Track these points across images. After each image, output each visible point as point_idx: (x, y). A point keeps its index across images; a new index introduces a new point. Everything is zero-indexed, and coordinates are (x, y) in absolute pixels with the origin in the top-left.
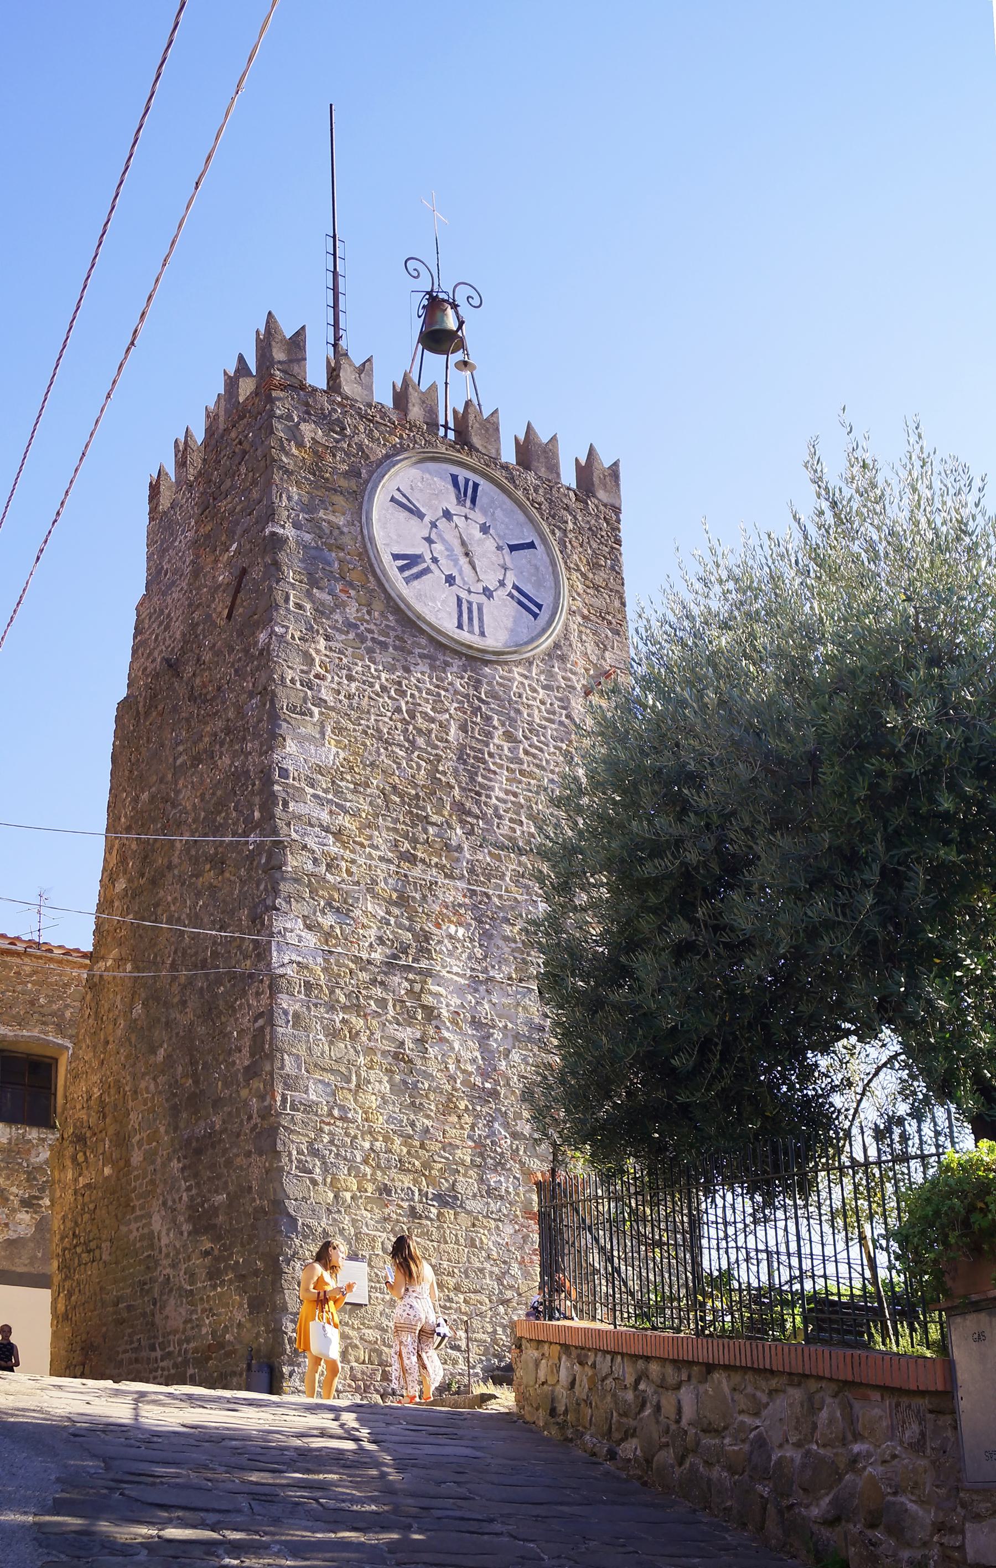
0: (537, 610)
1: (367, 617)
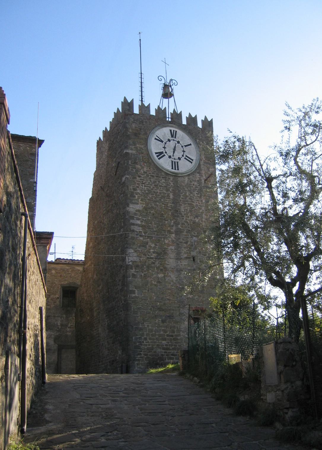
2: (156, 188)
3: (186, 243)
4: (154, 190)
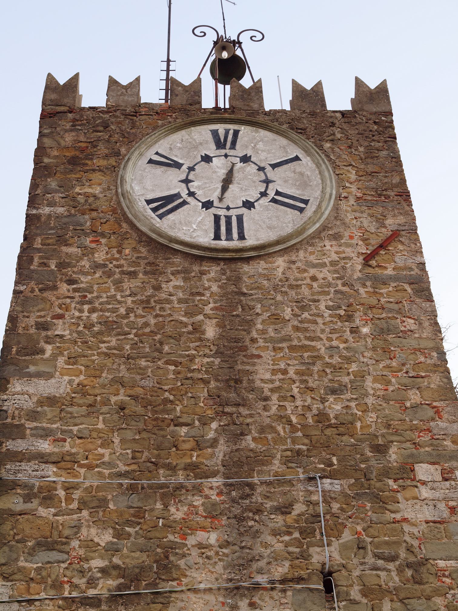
0: (303, 205)
1: (117, 256)
2: (140, 312)
3: (285, 509)
4: (132, 319)
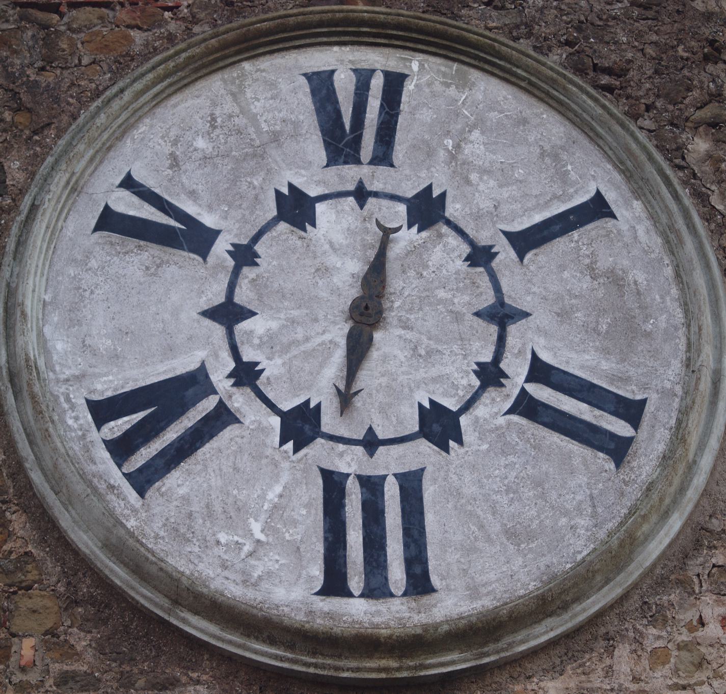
0: (621, 428)
